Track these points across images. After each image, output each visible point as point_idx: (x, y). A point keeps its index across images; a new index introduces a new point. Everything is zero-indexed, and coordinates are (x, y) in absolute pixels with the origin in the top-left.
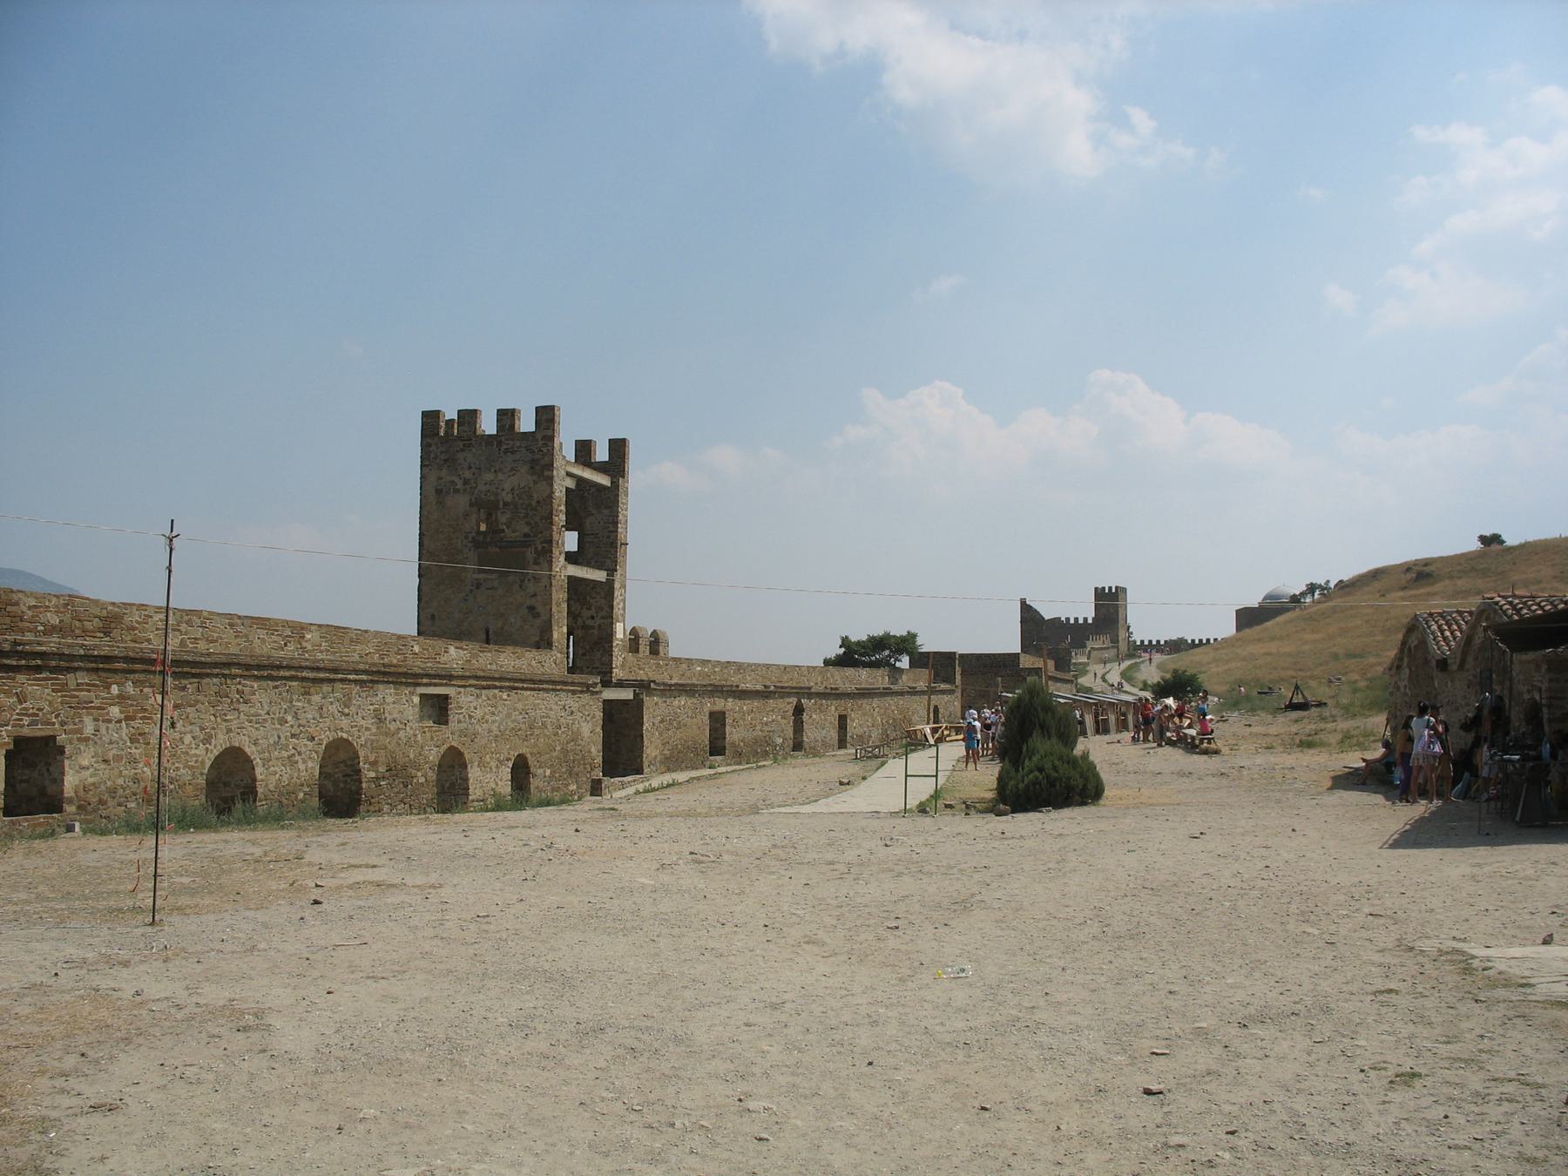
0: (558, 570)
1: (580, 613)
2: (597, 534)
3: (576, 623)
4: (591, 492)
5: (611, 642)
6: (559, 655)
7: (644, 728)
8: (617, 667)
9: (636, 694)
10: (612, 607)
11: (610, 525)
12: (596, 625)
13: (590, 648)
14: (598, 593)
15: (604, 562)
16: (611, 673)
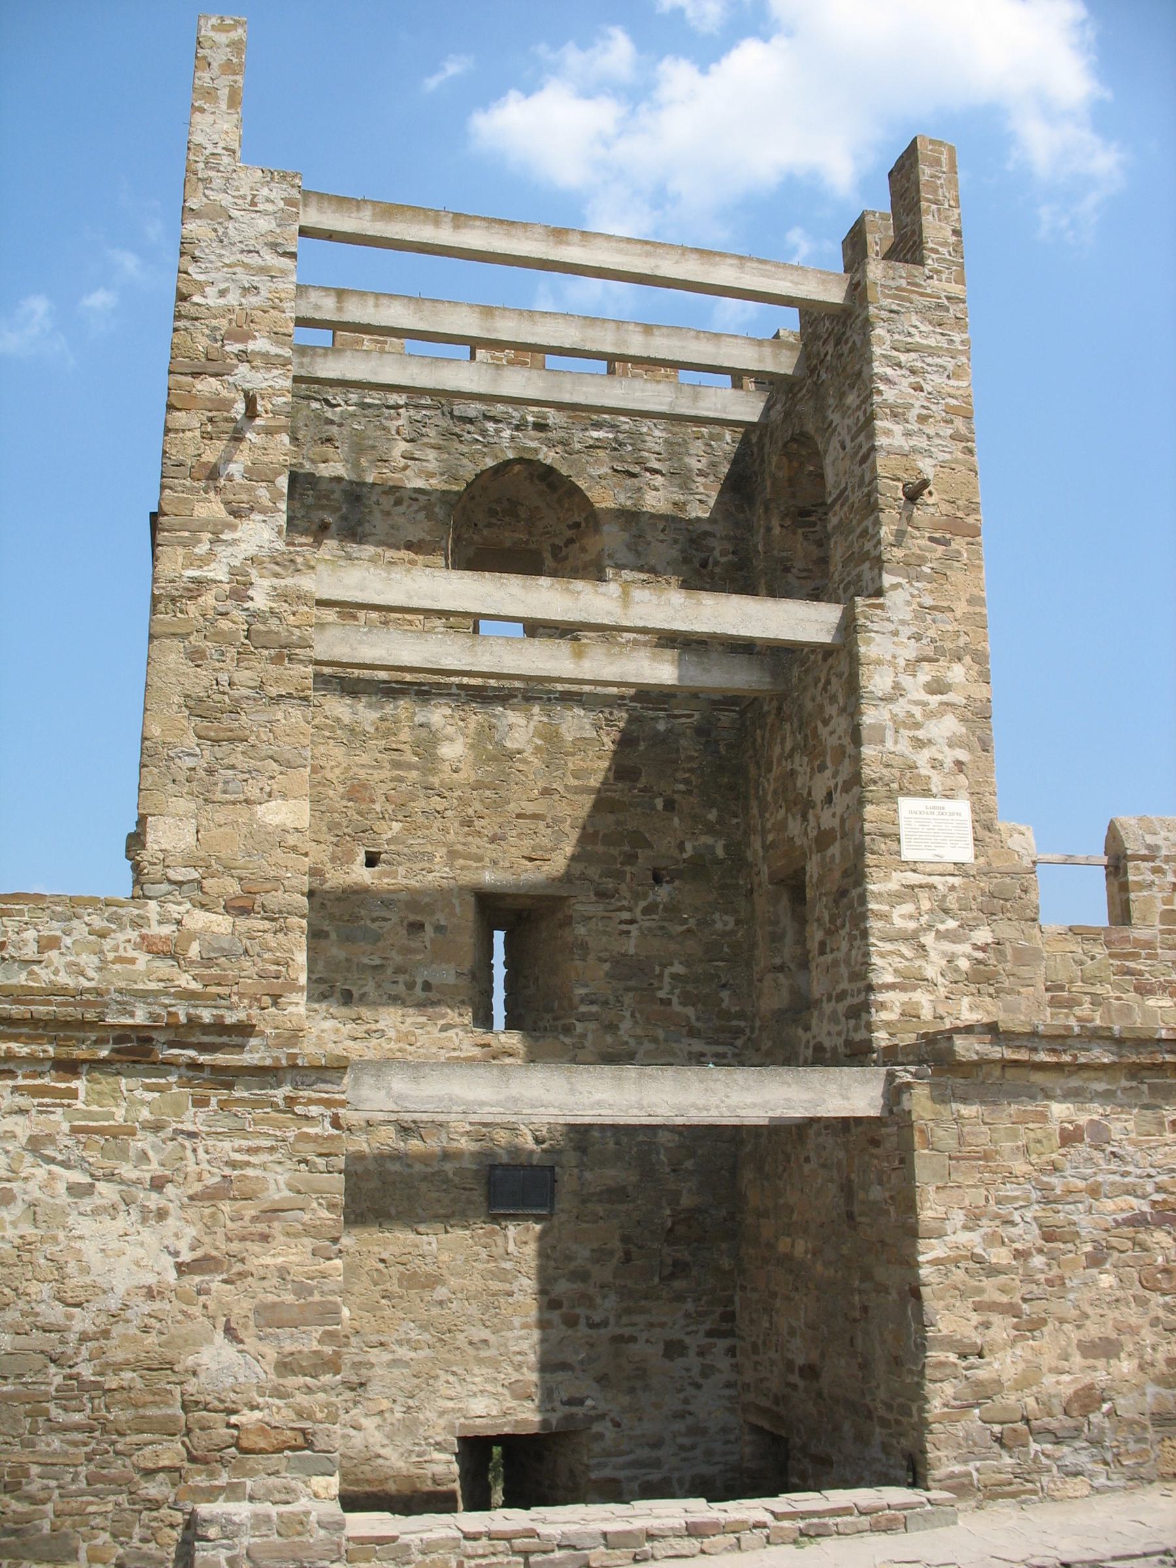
0: (218, 572)
1: (809, 794)
2: (846, 488)
3: (806, 833)
4: (829, 358)
5: (856, 875)
6: (221, 923)
7: (930, 1251)
8: (911, 981)
9: (895, 1093)
10: (856, 736)
11: (861, 438)
12: (836, 823)
13: (833, 919)
14: (833, 699)
15: (859, 576)
16: (866, 1006)
